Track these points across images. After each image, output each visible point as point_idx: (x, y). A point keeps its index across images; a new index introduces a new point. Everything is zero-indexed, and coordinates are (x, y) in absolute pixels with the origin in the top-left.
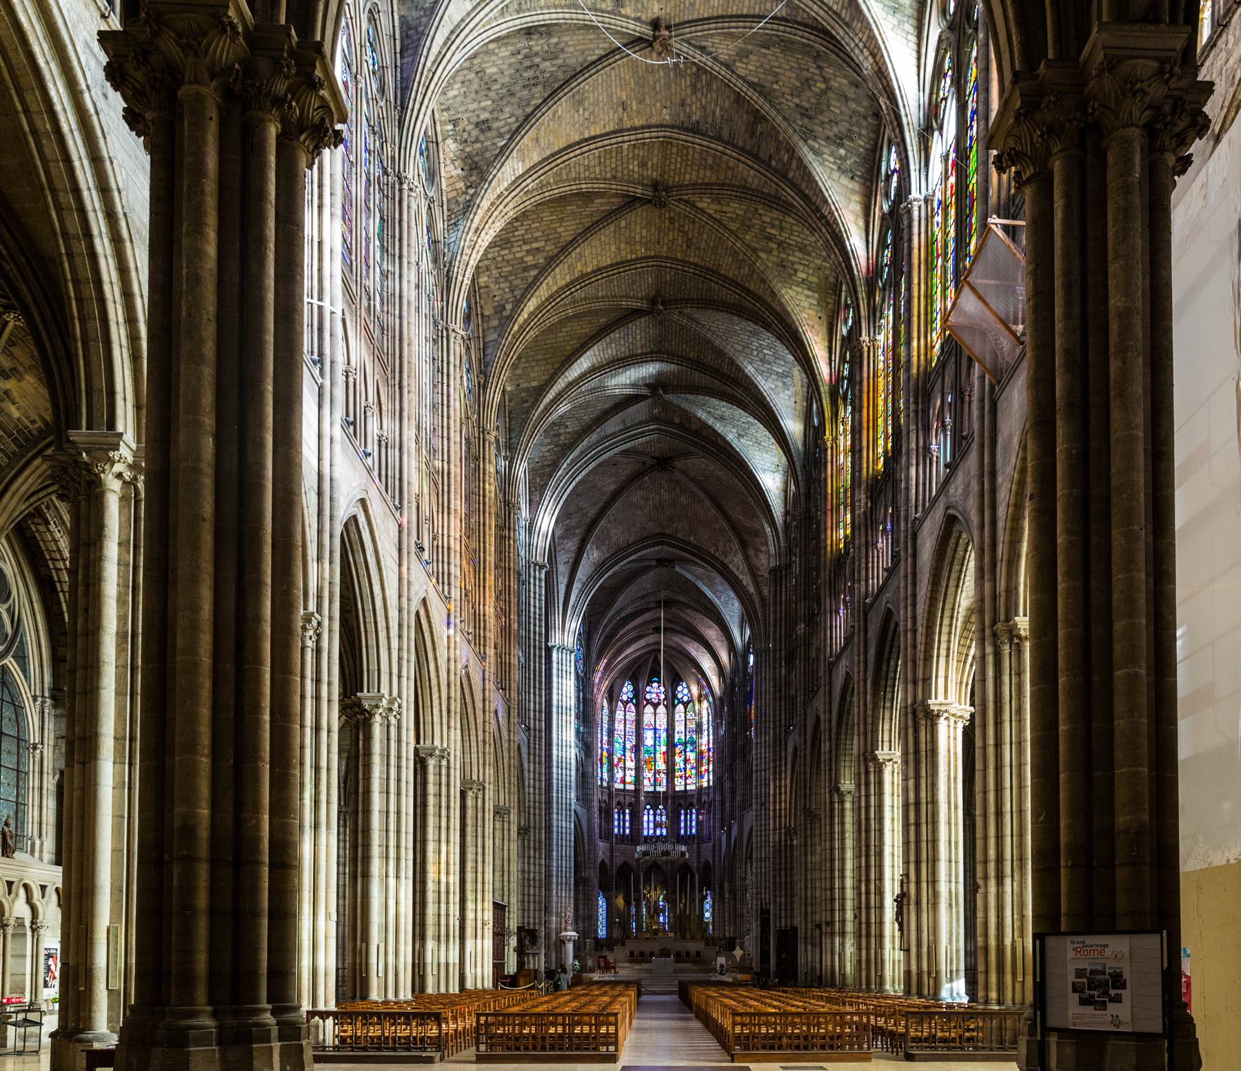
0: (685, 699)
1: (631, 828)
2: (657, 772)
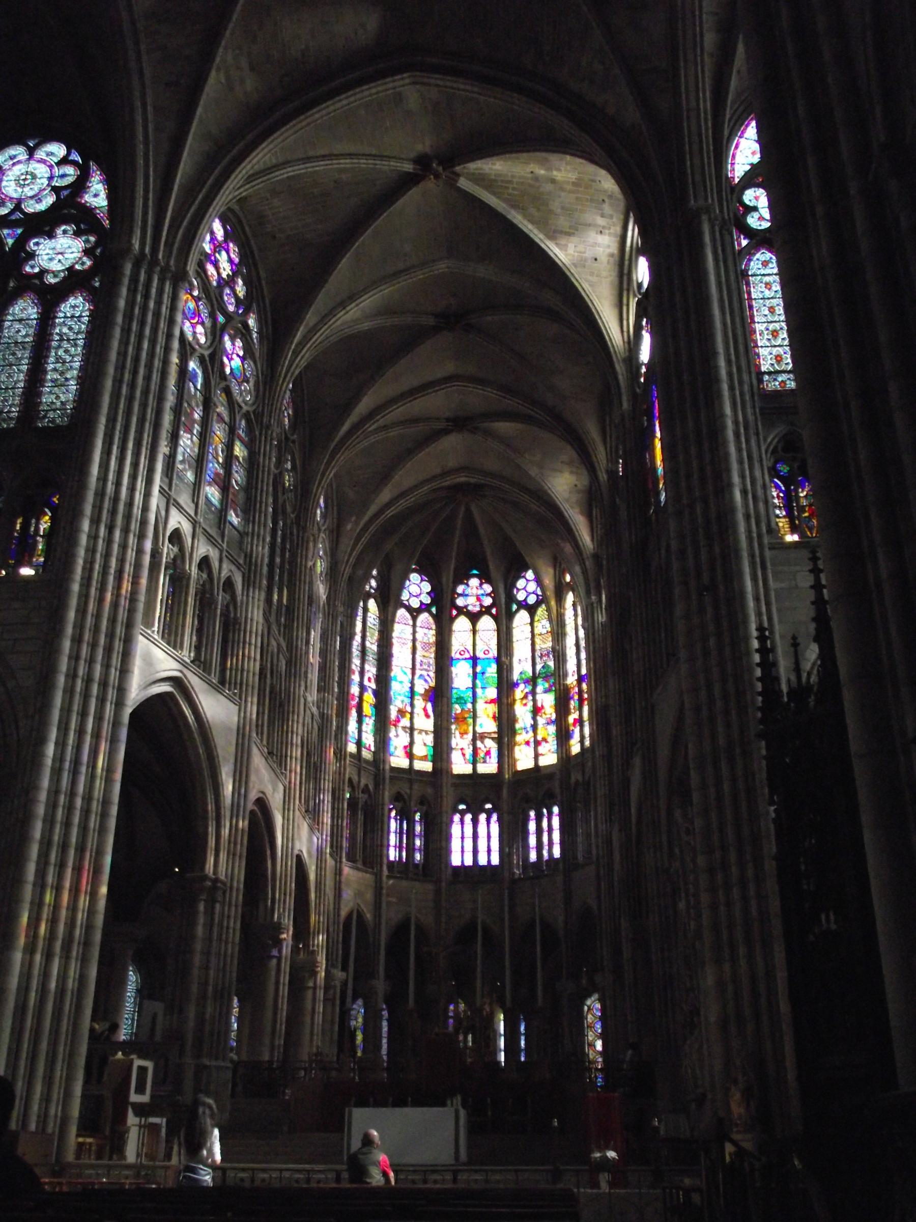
0: (532, 600)
2: (477, 737)
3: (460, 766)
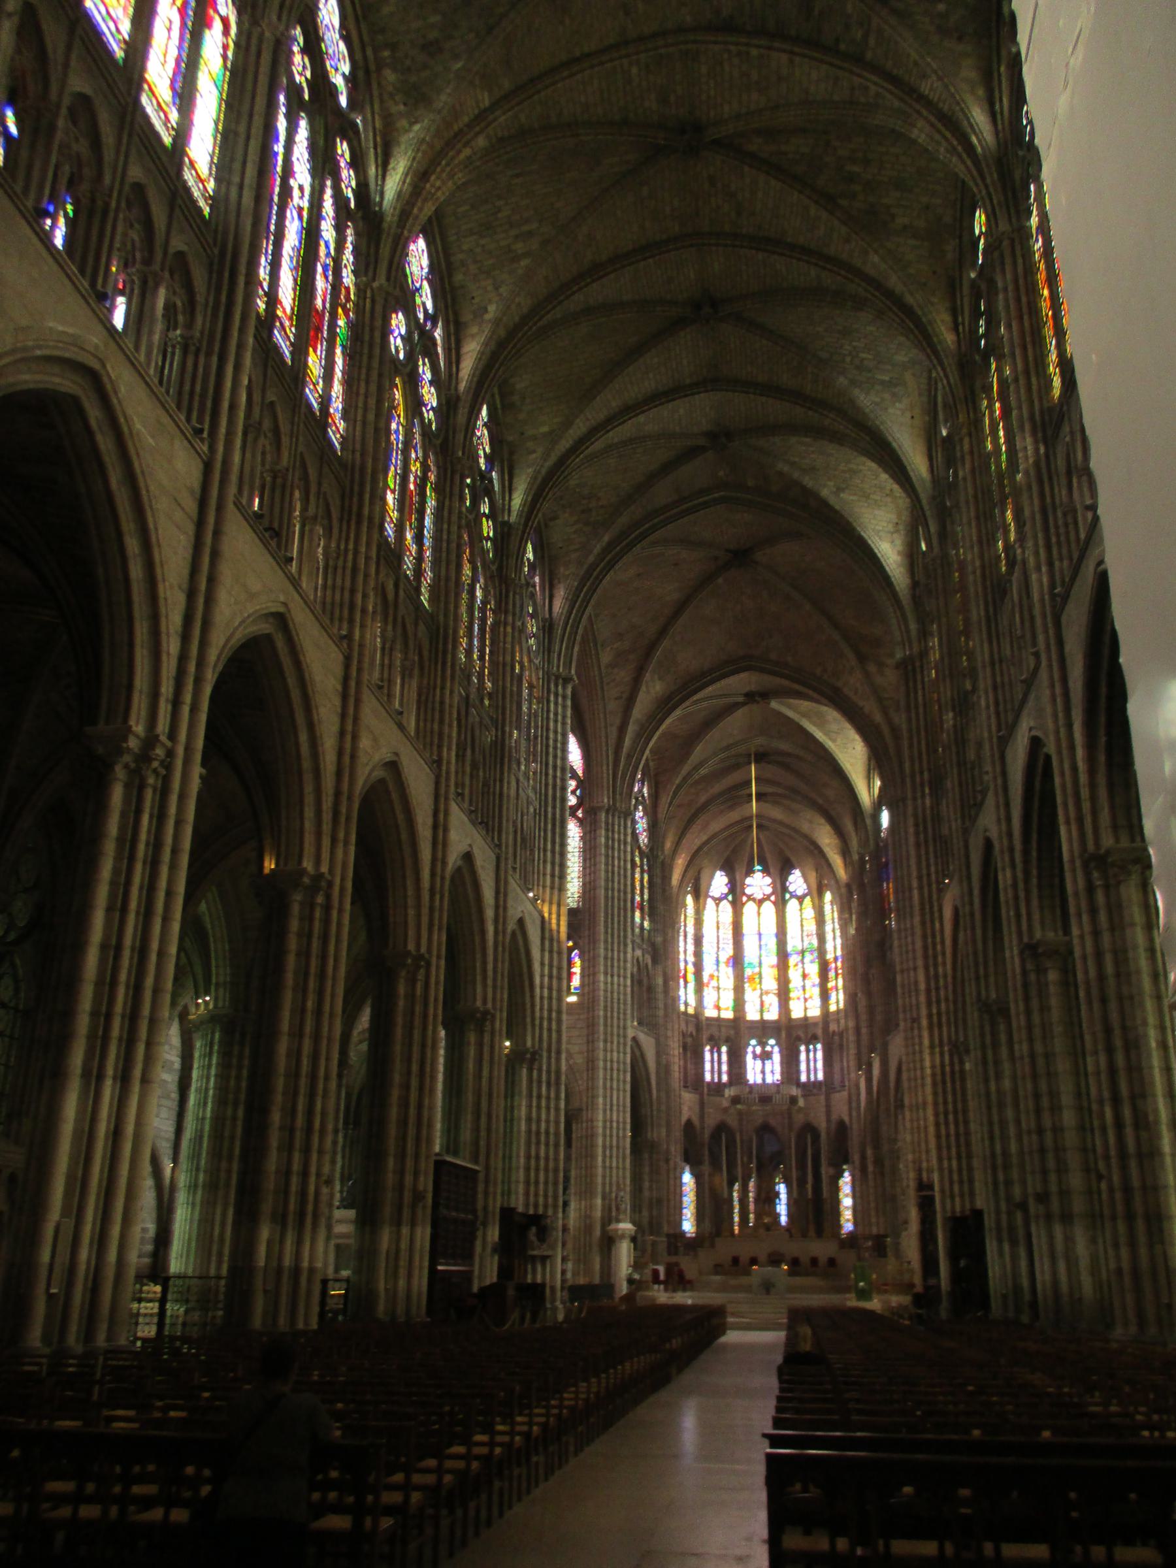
0: (800, 893)
1: (729, 1073)
3: (752, 1014)
